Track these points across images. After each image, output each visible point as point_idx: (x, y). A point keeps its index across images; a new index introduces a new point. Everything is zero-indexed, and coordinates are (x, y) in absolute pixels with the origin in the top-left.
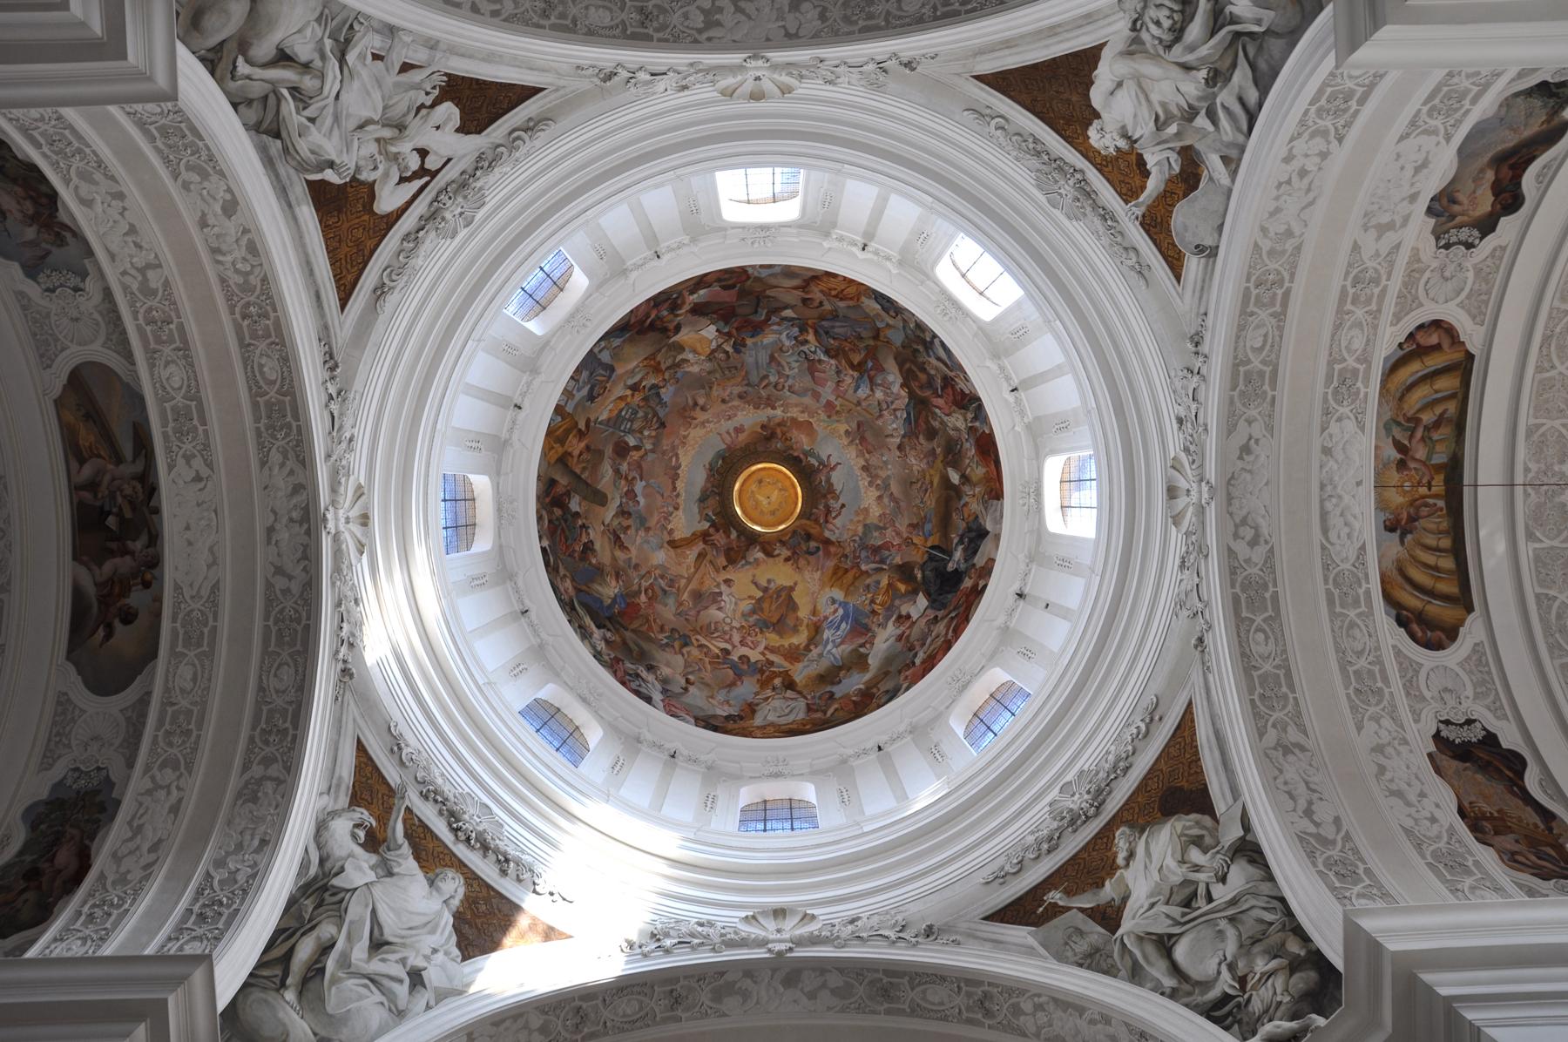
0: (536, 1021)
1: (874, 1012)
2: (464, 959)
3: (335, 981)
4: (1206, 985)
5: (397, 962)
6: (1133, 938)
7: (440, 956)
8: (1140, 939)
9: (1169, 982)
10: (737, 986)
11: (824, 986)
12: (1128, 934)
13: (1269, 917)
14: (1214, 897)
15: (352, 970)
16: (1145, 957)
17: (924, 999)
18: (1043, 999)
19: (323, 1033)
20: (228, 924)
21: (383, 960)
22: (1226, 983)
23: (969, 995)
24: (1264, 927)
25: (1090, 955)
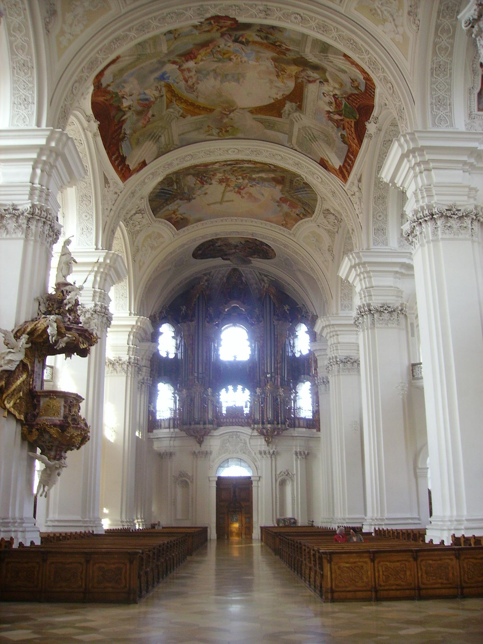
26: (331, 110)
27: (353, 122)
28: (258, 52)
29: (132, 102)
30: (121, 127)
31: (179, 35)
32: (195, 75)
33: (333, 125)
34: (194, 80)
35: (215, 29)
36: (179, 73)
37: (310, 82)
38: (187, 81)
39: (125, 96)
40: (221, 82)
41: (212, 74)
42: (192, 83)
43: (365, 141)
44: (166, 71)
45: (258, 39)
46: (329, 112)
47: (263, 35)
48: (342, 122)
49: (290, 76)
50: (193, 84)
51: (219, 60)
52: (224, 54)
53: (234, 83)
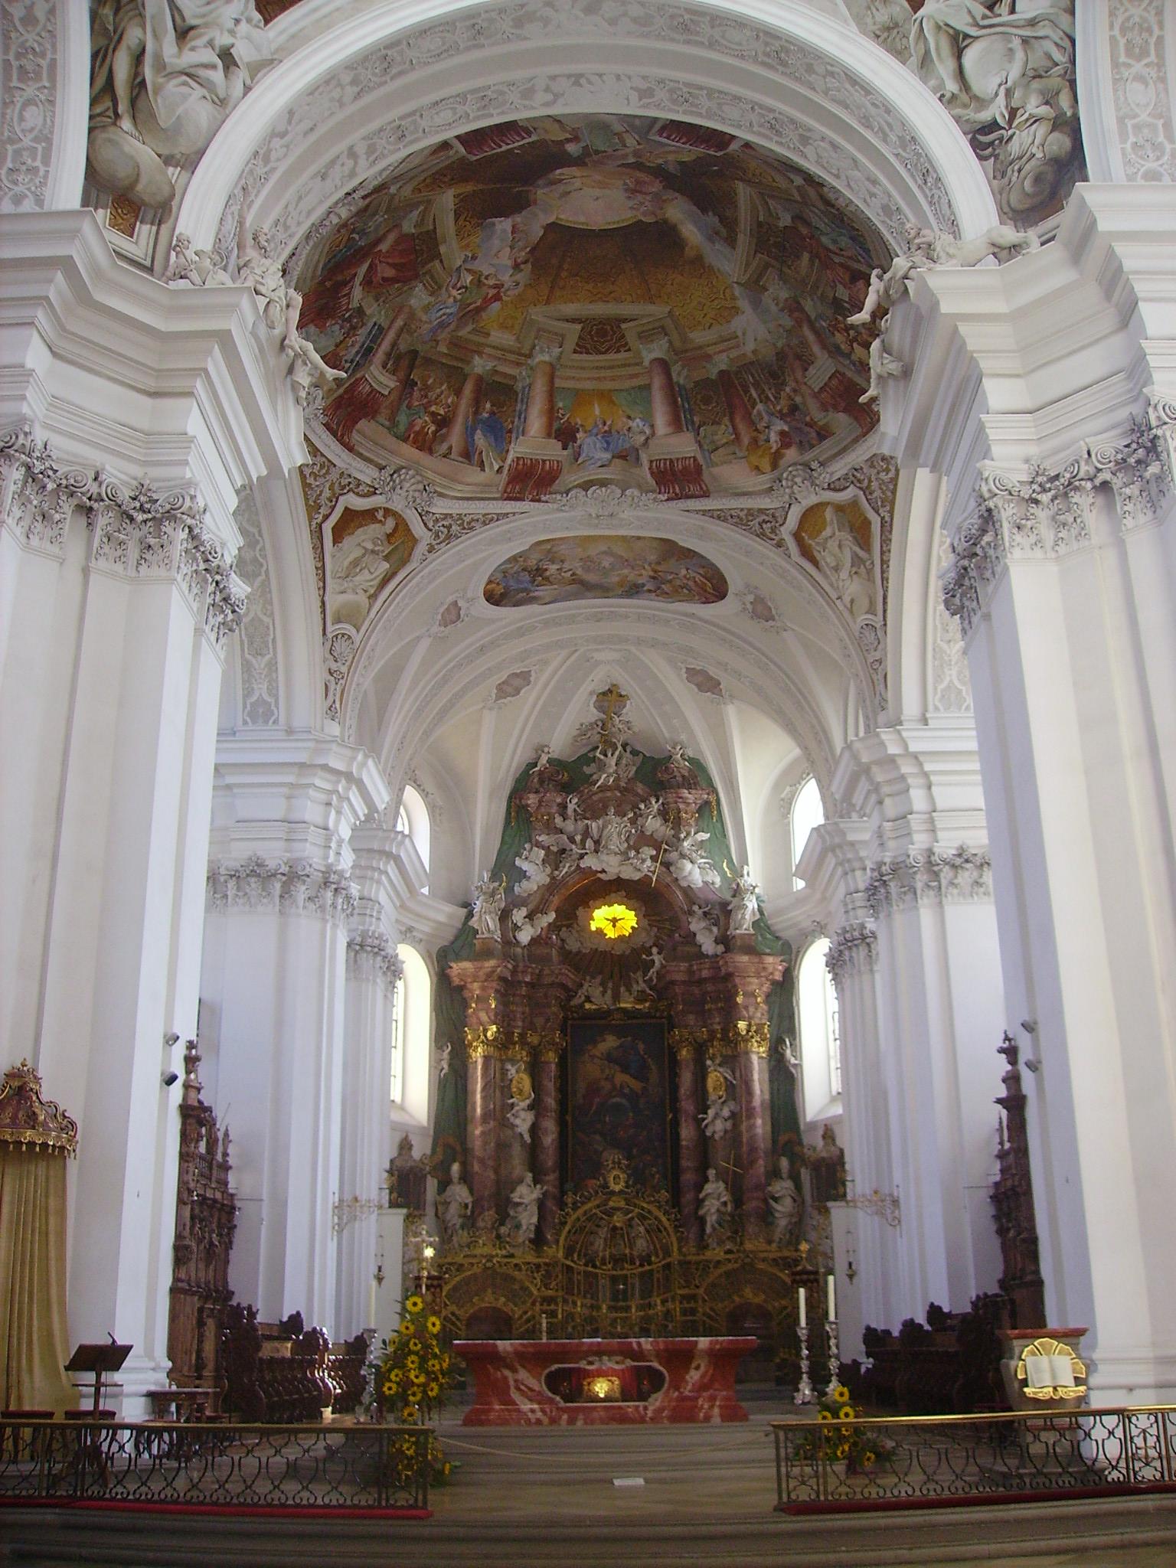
0: (346, 78)
1: (673, 40)
2: (267, 22)
3: (157, 90)
4: (981, 103)
5: (205, 46)
6: (932, 23)
7: (244, 27)
8: (938, 27)
9: (952, 86)
10: (538, 14)
11: (625, 14)
12: (930, 17)
13: (1058, 56)
14: (1017, 9)
15: (169, 70)
16: (937, 49)
17: (723, 37)
18: (834, 69)
19: (165, 152)
20: (52, 78)
21: (193, 49)
22: (997, 110)
23: (767, 44)
24: (1050, 64)
25: (889, 29)
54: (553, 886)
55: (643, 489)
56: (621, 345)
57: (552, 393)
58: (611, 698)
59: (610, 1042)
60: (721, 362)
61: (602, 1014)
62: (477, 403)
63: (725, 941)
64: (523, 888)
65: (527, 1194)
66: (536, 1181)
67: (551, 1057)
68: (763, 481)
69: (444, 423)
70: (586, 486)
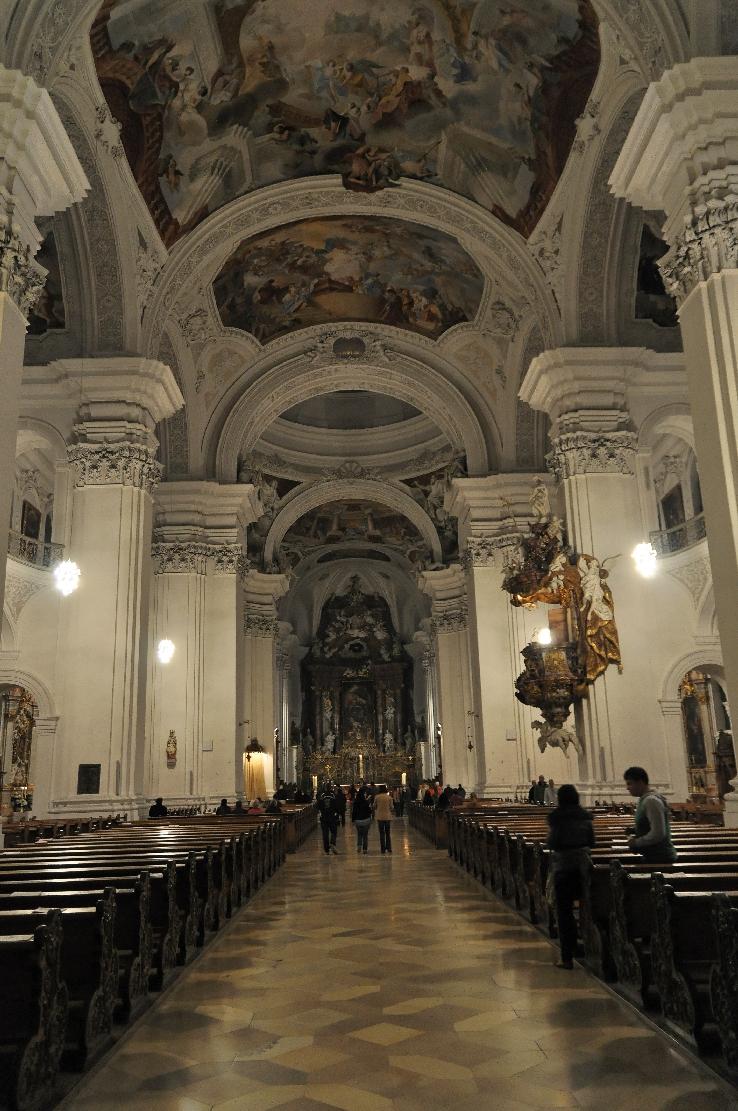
4: (440, 522)
26: (169, 55)
27: (130, 86)
28: (309, 97)
29: (525, 71)
30: (558, 57)
31: (419, 161)
32: (412, 44)
33: (153, 39)
34: (415, 32)
35: (372, 154)
36: (437, 63)
37: (220, 73)
38: (428, 35)
39: (526, 98)
40: (367, 17)
41: (384, 36)
42: (421, 27)
43: (101, 100)
44: (456, 82)
45: (315, 132)
46: (170, 48)
47: (308, 147)
48: (143, 62)
49: (251, 60)
50: (418, 24)
51: (369, 66)
52: (360, 85)
53: (347, 13)
54: (338, 639)
55: (365, 540)
56: (360, 509)
57: (340, 519)
58: (355, 579)
59: (355, 688)
60: (387, 514)
61: (353, 678)
62: (318, 523)
63: (390, 656)
64: (329, 640)
65: (330, 738)
66: (334, 734)
67: (337, 694)
68: (400, 542)
69: (308, 529)
70: (349, 540)
